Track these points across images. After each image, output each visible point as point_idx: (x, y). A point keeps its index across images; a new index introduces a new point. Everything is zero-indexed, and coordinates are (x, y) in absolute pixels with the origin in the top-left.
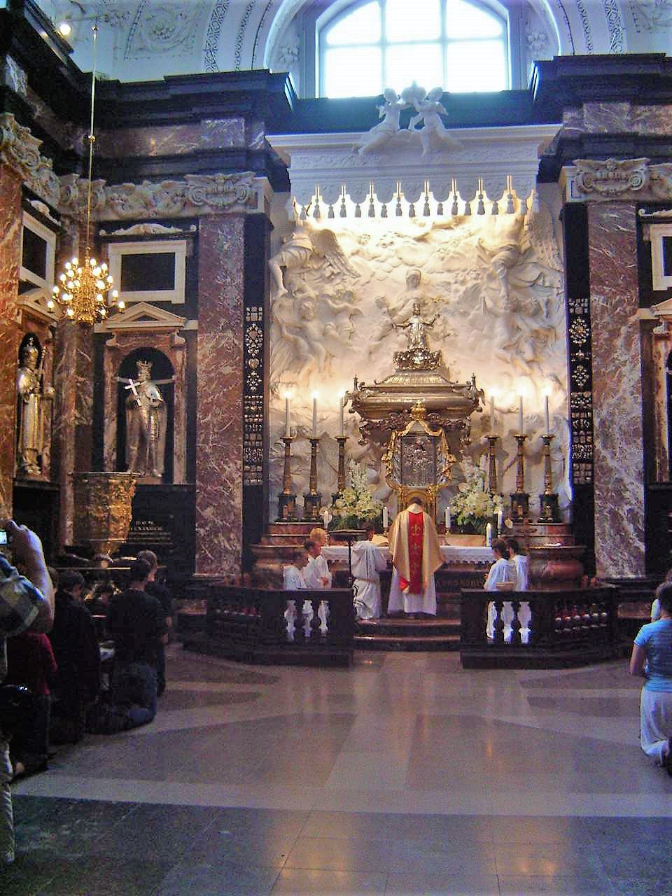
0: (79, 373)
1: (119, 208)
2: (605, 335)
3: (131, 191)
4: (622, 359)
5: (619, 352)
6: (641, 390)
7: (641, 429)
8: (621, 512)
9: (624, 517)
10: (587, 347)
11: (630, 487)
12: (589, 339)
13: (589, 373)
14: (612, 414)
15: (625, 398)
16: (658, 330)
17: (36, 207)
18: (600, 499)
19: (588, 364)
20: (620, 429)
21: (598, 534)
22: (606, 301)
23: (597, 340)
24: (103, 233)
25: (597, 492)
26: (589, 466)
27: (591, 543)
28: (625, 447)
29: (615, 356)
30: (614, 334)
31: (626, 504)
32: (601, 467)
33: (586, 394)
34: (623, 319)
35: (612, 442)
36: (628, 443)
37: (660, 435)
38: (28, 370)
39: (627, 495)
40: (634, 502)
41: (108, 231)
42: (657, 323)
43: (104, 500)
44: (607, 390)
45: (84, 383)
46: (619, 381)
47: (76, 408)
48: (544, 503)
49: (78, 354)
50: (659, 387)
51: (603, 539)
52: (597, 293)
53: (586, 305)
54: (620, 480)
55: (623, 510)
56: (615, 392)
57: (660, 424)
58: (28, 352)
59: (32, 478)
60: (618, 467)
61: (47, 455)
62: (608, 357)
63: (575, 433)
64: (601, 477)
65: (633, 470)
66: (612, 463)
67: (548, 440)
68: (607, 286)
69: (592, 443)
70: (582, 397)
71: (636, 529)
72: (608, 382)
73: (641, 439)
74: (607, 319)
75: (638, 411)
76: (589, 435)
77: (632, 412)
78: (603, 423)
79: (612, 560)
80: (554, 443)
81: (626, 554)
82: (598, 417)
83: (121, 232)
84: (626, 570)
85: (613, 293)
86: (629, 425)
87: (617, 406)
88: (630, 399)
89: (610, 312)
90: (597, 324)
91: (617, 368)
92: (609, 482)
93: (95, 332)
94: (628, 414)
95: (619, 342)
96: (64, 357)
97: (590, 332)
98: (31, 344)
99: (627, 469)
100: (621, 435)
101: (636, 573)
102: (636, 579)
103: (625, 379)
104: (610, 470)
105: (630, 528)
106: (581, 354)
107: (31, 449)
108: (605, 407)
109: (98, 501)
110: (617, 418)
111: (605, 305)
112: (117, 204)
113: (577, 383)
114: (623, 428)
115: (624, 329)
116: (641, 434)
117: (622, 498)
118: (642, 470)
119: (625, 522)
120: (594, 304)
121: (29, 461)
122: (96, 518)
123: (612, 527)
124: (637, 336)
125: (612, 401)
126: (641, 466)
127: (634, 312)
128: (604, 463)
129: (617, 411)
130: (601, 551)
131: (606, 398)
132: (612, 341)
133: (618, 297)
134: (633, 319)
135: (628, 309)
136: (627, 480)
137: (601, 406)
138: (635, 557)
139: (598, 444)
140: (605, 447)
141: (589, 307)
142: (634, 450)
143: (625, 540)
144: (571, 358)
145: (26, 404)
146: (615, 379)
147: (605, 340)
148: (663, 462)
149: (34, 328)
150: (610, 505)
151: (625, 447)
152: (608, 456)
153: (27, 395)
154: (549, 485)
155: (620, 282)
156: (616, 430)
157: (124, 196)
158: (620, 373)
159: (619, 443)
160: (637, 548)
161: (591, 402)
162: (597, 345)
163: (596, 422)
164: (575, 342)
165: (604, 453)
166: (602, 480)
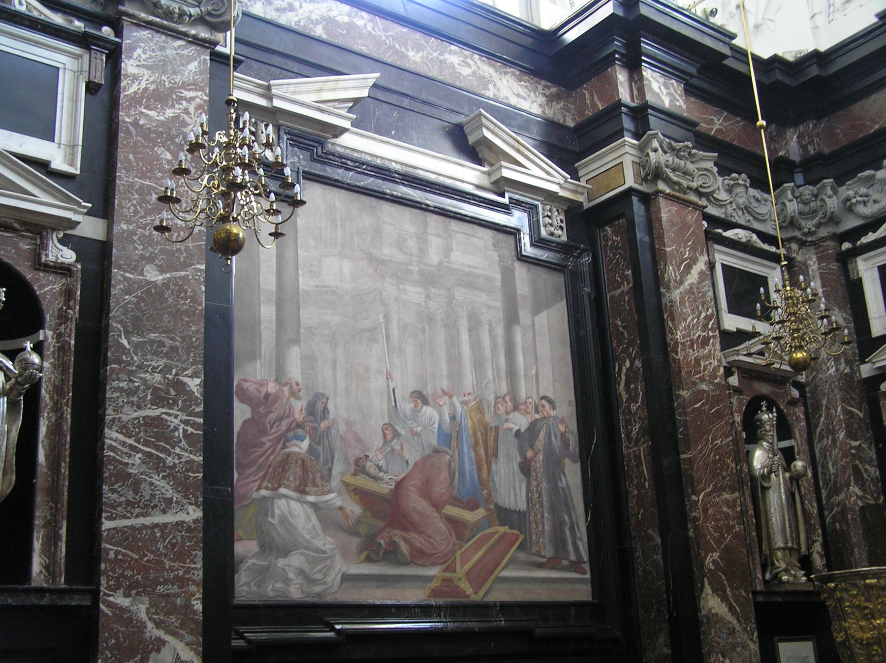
0: (851, 435)
1: (861, 209)
3: (870, 181)
17: (736, 238)
24: (846, 246)
38: (765, 443)
41: (854, 242)
43: (866, 611)
45: (859, 448)
47: (856, 483)
49: (846, 412)
58: (760, 420)
59: (788, 588)
61: (818, 553)
83: (864, 240)
93: (864, 376)
96: (822, 419)
98: (764, 409)
107: (784, 549)
109: (857, 614)
112: (855, 204)
121: (783, 565)
122: (860, 641)
145: (765, 489)
149: (765, 389)
153: (766, 477)
157: (863, 190)
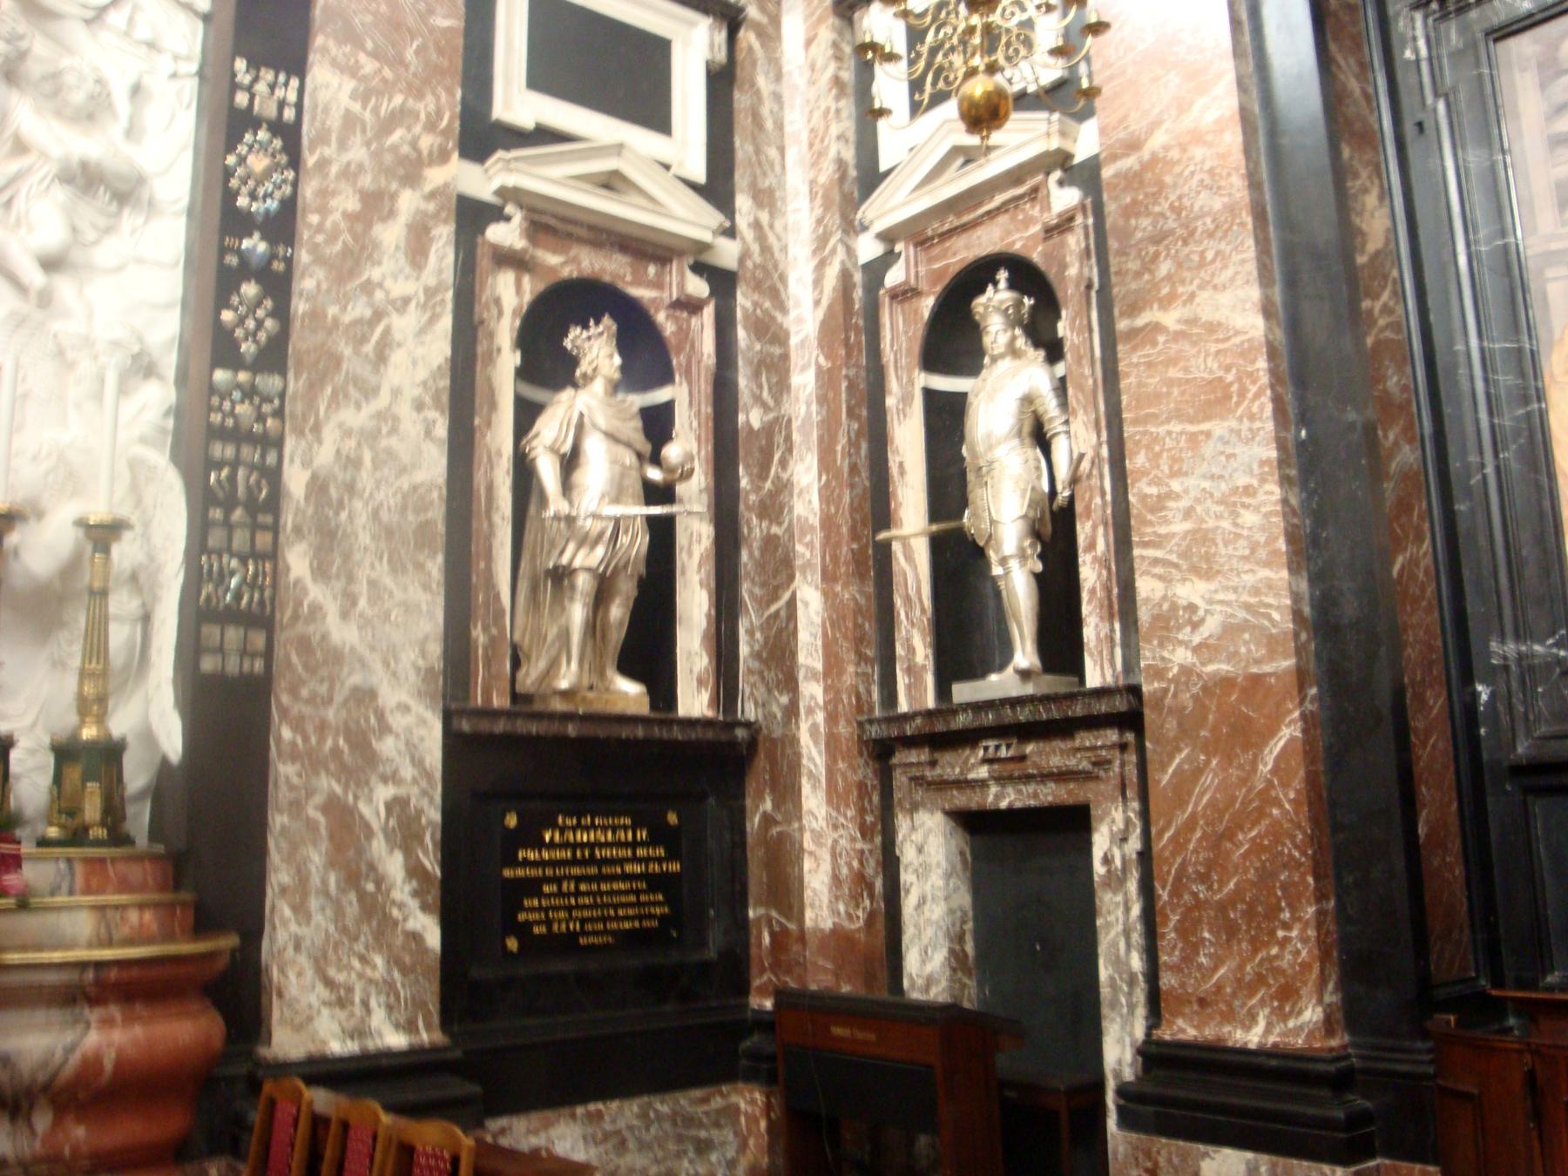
2: (347, 202)
4: (400, 288)
5: (387, 266)
6: (445, 399)
7: (441, 528)
8: (364, 809)
9: (376, 825)
10: (282, 225)
11: (398, 721)
12: (290, 207)
13: (282, 312)
14: (357, 463)
15: (396, 419)
16: (506, 234)
18: (294, 756)
19: (278, 286)
20: (375, 515)
21: (284, 890)
22: (364, 96)
23: (323, 210)
25: (286, 733)
26: (258, 640)
27: (252, 927)
28: (388, 581)
29: (375, 274)
30: (376, 205)
31: (385, 779)
32: (304, 645)
33: (271, 383)
34: (410, 170)
35: (347, 557)
36: (397, 567)
37: (489, 557)
39: (387, 747)
40: (408, 772)
42: (494, 213)
44: (340, 378)
46: (381, 358)
48: (74, 774)
50: (493, 405)
51: (301, 910)
52: (334, 63)
53: (292, 96)
54: (365, 696)
55: (374, 805)
56: (370, 392)
57: (491, 524)
60: (362, 650)
62: (352, 273)
63: (217, 514)
64: (303, 682)
65: (409, 658)
66: (343, 633)
67: (103, 535)
68: (369, 54)
69: (274, 555)
70: (250, 392)
71: (414, 870)
72: (347, 351)
73: (440, 558)
74: (357, 153)
75: (433, 466)
76: (265, 528)
77: (415, 466)
78: (318, 486)
79: (329, 983)
80: (125, 553)
81: (379, 960)
82: (306, 464)
84: (378, 1018)
85: (384, 81)
86: (404, 509)
87: (371, 436)
88: (411, 423)
89: (369, 134)
90: (323, 164)
91: (378, 315)
92: (328, 700)
94: (403, 471)
95: (391, 234)
97: (295, 184)
99: (390, 657)
100: (373, 537)
101: (410, 1027)
102: (413, 1051)
103: (398, 357)
104: (336, 657)
105: (394, 865)
106: (255, 245)
108: (330, 434)
110: (365, 479)
111: (356, 107)
113: (235, 345)
114: (385, 515)
115: (409, 202)
116: (441, 541)
117: (370, 758)
118: (438, 665)
119: (378, 846)
120: (323, 96)
123: (331, 864)
124: (444, 235)
125: (356, 417)
126: (436, 649)
127: (442, 157)
128: (311, 629)
129: (367, 457)
130: (290, 951)
131: (335, 403)
132: (369, 226)
133: (398, 100)
134: (436, 176)
135: (427, 142)
136: (389, 696)
137: (317, 429)
138: (405, 971)
139: (298, 561)
140: (321, 571)
141: (299, 106)
142: (418, 595)
143: (375, 910)
144: (223, 251)
146: (369, 348)
147: (346, 215)
148: (493, 643)
150: (327, 784)
151: (388, 581)
152: (332, 609)
154: (93, 705)
155: (410, 54)
156: (362, 519)
158: (387, 331)
159: (371, 567)
160: (416, 937)
161: (279, 413)
162: (319, 228)
163: (296, 480)
164: (242, 202)
165: (316, 592)
166: (304, 692)
